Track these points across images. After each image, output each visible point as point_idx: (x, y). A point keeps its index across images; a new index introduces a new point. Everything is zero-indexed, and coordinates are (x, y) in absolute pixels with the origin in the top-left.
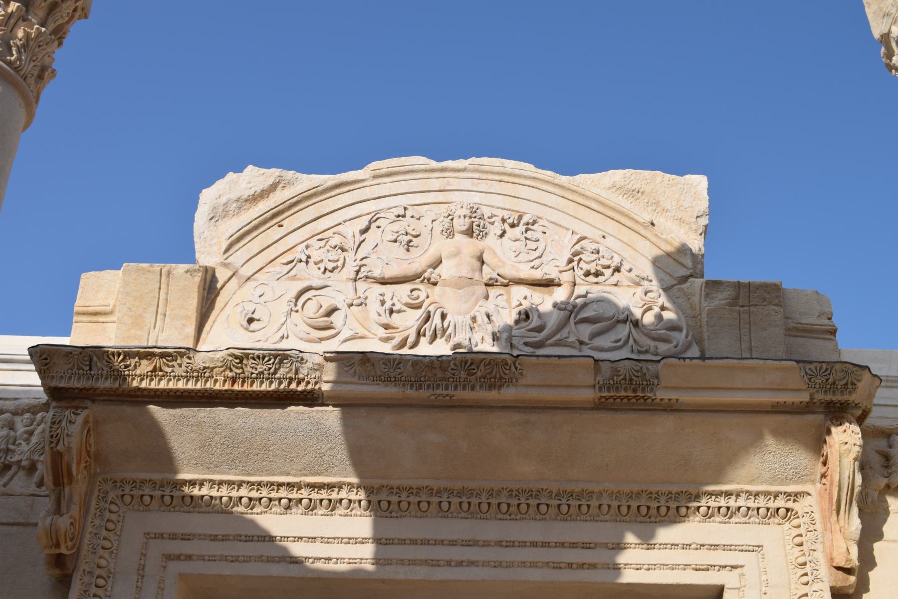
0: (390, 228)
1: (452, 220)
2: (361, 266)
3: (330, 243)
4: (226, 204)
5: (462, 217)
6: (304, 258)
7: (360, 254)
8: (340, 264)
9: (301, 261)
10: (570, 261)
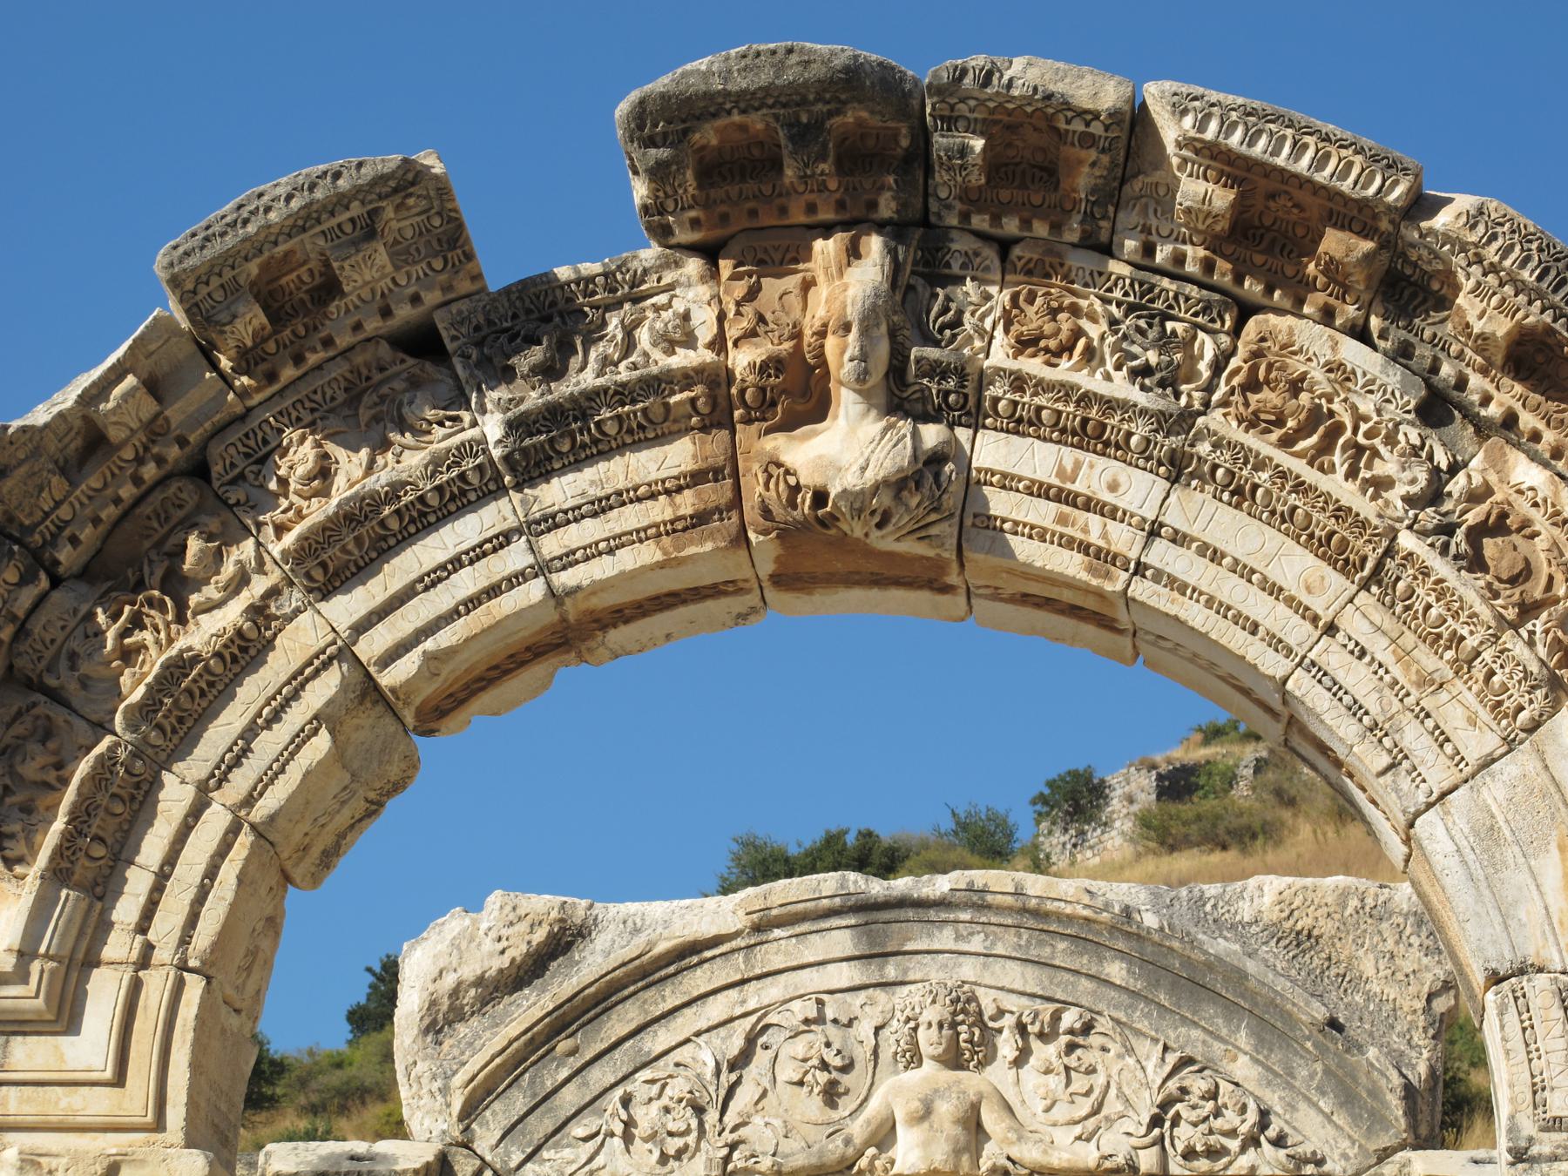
0: (790, 1054)
1: (915, 1029)
2: (733, 1147)
3: (668, 1091)
4: (455, 993)
5: (935, 1027)
6: (618, 1128)
7: (731, 1118)
8: (691, 1139)
9: (612, 1135)
10: (1156, 1121)
